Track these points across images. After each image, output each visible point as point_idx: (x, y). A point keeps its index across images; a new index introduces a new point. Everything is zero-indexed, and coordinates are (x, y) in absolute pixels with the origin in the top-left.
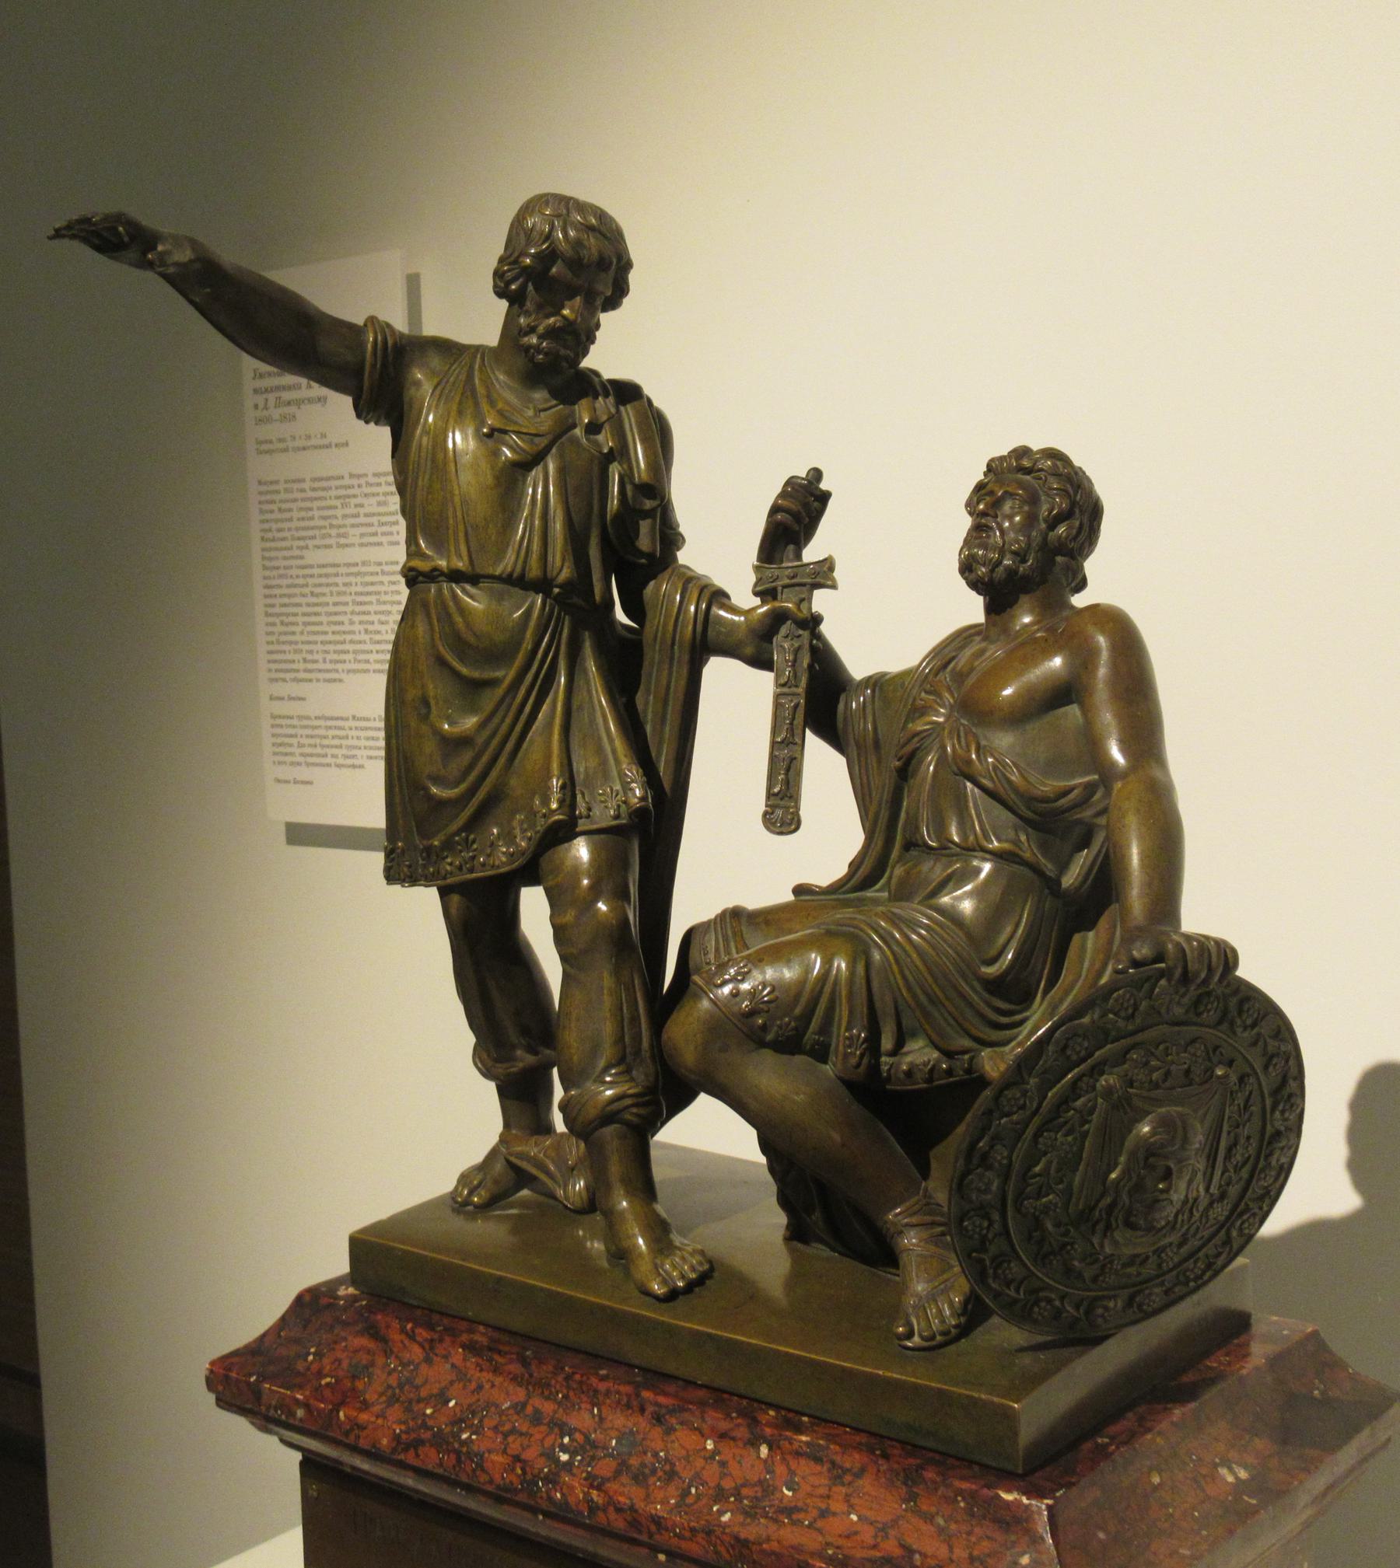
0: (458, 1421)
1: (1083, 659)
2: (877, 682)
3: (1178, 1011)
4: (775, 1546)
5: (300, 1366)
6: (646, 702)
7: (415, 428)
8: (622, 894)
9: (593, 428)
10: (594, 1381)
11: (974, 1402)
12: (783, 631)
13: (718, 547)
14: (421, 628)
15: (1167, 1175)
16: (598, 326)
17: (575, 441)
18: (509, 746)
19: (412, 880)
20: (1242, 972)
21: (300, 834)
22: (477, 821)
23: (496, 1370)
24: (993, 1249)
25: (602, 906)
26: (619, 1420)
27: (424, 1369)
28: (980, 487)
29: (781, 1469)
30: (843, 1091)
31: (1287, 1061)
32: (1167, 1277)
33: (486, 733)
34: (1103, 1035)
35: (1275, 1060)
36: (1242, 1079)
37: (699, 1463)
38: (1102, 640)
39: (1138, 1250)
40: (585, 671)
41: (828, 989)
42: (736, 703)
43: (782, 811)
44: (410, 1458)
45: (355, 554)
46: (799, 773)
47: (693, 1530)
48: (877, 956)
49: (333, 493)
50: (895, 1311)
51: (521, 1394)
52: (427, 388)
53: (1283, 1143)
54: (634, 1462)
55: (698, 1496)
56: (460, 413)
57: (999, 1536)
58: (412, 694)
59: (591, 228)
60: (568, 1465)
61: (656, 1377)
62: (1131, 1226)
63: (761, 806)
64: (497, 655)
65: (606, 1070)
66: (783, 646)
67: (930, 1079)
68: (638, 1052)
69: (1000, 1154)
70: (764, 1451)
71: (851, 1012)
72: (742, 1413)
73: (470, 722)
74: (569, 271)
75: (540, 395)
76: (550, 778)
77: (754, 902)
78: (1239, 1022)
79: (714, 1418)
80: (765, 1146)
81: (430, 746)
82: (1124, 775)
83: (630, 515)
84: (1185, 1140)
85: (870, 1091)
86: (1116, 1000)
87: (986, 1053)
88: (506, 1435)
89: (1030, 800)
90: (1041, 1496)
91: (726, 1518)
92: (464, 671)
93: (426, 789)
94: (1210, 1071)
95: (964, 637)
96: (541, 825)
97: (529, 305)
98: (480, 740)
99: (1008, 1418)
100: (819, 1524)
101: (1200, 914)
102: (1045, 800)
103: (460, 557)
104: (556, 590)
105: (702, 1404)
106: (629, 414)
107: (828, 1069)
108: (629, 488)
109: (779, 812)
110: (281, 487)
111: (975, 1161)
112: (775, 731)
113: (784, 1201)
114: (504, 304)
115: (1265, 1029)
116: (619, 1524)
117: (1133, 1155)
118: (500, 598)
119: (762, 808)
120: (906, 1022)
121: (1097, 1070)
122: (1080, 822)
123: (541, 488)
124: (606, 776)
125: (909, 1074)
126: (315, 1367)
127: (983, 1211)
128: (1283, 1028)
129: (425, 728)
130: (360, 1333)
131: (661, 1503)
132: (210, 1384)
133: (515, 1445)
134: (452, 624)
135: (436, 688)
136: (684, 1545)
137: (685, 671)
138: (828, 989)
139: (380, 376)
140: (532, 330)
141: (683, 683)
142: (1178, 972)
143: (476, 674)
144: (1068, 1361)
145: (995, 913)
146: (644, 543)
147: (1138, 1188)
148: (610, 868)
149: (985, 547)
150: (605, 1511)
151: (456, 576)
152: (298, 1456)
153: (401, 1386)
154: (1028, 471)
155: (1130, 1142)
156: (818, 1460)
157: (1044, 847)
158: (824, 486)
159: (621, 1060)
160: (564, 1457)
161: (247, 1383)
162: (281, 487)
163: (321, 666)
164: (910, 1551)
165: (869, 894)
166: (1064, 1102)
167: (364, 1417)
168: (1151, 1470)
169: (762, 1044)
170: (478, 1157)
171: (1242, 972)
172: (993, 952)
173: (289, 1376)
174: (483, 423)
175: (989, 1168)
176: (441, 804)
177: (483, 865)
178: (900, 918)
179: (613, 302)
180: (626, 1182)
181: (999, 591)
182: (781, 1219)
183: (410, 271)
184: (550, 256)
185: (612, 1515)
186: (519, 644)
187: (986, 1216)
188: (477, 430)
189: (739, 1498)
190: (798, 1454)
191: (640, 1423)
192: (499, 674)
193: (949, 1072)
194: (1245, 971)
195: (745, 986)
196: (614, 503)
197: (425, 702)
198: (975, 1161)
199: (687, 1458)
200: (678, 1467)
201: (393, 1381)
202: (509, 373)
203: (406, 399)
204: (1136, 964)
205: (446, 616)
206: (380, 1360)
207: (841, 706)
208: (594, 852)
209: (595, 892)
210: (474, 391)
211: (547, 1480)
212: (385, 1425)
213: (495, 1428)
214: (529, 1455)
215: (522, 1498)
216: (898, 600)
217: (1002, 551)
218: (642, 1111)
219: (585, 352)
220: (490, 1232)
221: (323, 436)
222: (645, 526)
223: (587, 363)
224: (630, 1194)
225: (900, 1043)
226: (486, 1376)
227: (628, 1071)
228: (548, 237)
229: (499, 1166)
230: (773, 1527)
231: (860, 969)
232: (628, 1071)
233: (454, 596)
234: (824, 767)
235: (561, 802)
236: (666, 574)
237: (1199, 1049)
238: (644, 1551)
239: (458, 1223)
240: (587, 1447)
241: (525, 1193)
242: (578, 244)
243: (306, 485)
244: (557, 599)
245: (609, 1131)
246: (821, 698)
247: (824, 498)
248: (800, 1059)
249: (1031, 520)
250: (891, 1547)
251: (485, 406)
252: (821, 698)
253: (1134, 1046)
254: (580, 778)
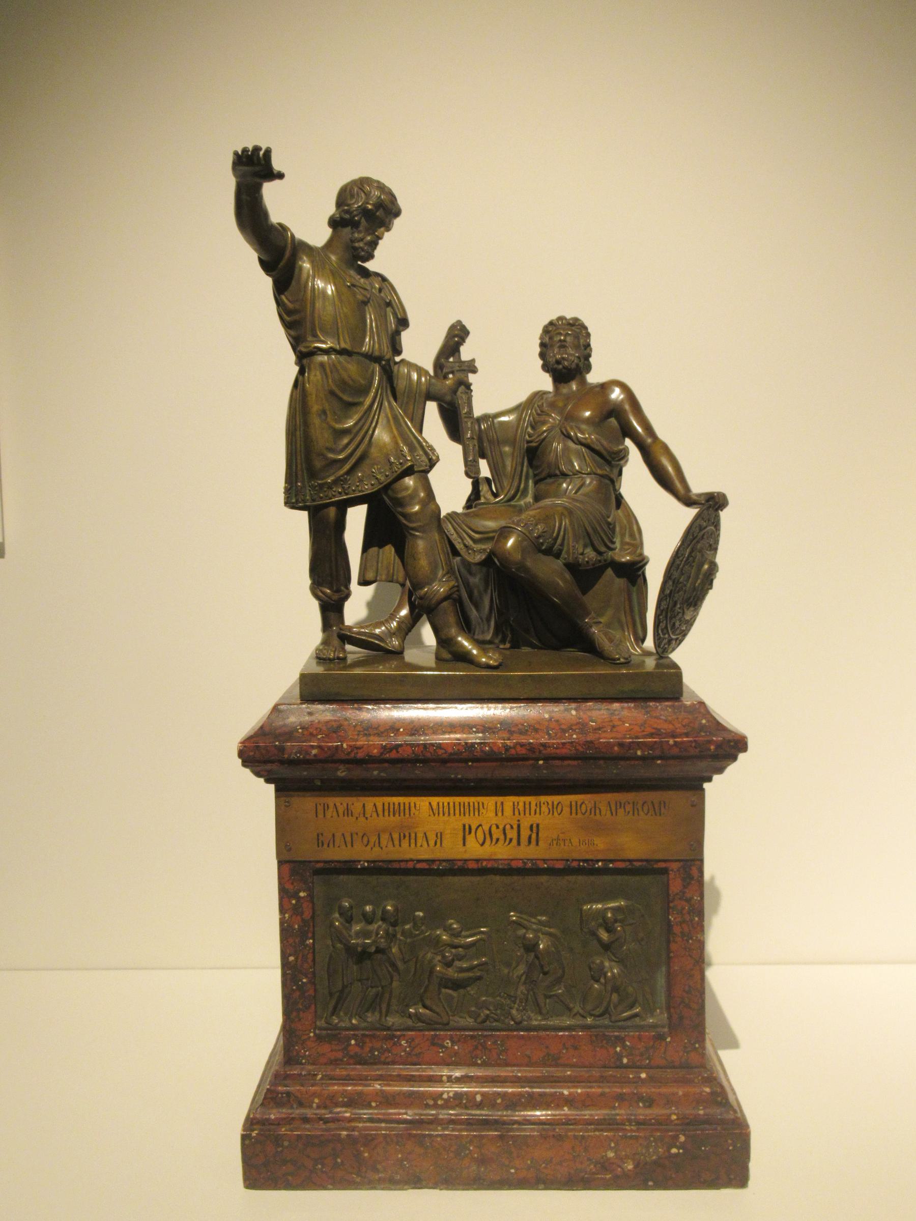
33: (358, 428)
65: (443, 577)
73: (350, 423)
81: (327, 434)
92: (346, 398)
97: (361, 228)
98: (355, 431)
100: (615, 730)
104: (384, 363)
107: (560, 562)
140: (362, 240)
143: (350, 400)
151: (342, 352)
159: (448, 573)
165: (512, 503)
169: (540, 551)
174: (344, 281)
177: (354, 491)
192: (361, 400)
203: (297, 266)
216: (507, 381)
245: (445, 604)
247: (467, 333)
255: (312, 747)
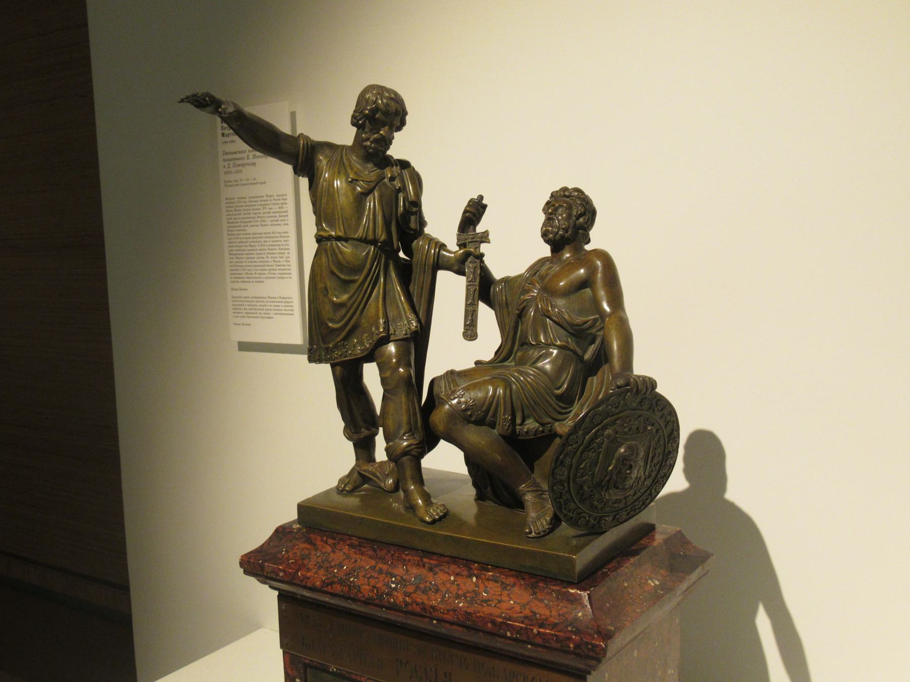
0: (348, 574)
1: (592, 270)
2: (506, 280)
3: (634, 405)
4: (481, 614)
5: (280, 556)
6: (414, 288)
7: (320, 178)
8: (408, 365)
9: (392, 179)
10: (404, 556)
11: (558, 556)
12: (469, 260)
13: (441, 224)
14: (324, 260)
15: (631, 467)
16: (393, 138)
17: (385, 184)
18: (361, 306)
19: (320, 361)
20: (657, 390)
21: (244, 347)
22: (347, 337)
23: (362, 554)
24: (564, 498)
25: (401, 370)
26: (414, 571)
27: (332, 555)
28: (548, 203)
29: (481, 585)
30: (502, 440)
33: (351, 302)
34: (608, 415)
36: (657, 431)
37: (448, 585)
38: (599, 263)
40: (390, 276)
41: (495, 400)
42: (451, 289)
43: (470, 332)
44: (329, 589)
45: (270, 229)
46: (477, 317)
47: (448, 611)
48: (514, 387)
49: (259, 203)
50: (524, 524)
51: (373, 563)
52: (324, 162)
54: (422, 586)
55: (449, 597)
56: (339, 172)
57: (570, 606)
58: (320, 286)
59: (392, 99)
60: (395, 589)
61: (429, 554)
62: (616, 487)
63: (461, 329)
64: (356, 270)
65: (404, 435)
66: (469, 266)
67: (535, 435)
68: (416, 428)
69: (568, 461)
70: (474, 579)
71: (505, 410)
72: (465, 566)
73: (345, 297)
74: (381, 115)
75: (370, 165)
76: (379, 319)
77: (458, 368)
79: (453, 568)
80: (468, 461)
81: (328, 307)
82: (610, 315)
83: (407, 214)
84: (638, 454)
85: (512, 439)
87: (556, 424)
88: (368, 579)
89: (572, 325)
90: (584, 590)
91: (461, 605)
92: (342, 277)
93: (327, 324)
94: (645, 428)
95: (542, 262)
96: (376, 338)
97: (366, 130)
98: (349, 304)
99: (572, 562)
101: (640, 368)
102: (577, 325)
103: (340, 231)
105: (448, 563)
106: (406, 173)
107: (496, 431)
108: (407, 203)
109: (469, 332)
110: (236, 200)
112: (467, 299)
113: (475, 484)
114: (355, 129)
115: (666, 412)
116: (418, 609)
117: (618, 460)
118: (356, 247)
119: (462, 330)
120: (526, 413)
121: (605, 428)
122: (591, 334)
123: (371, 203)
124: (401, 317)
125: (527, 432)
126: (286, 556)
127: (561, 482)
129: (326, 300)
130: (304, 542)
131: (435, 600)
132: (242, 564)
133: (373, 582)
134: (337, 257)
135: (330, 283)
136: (445, 616)
137: (430, 277)
138: (495, 400)
139: (304, 157)
140: (368, 139)
141: (429, 281)
142: (635, 390)
143: (347, 278)
144: (592, 541)
145: (559, 370)
146: (413, 225)
147: (619, 472)
148: (403, 356)
149: (552, 227)
150: (411, 605)
151: (338, 239)
152: (277, 593)
153: (323, 562)
154: (568, 197)
155: (617, 455)
156: (496, 582)
157: (578, 344)
158: (484, 202)
159: (410, 430)
160: (393, 586)
161: (256, 565)
162: (236, 200)
163: (254, 276)
164: (535, 613)
165: (506, 364)
166: (592, 440)
167: (309, 574)
169: (470, 422)
170: (346, 472)
171: (657, 390)
172: (559, 385)
173: (275, 559)
174: (348, 177)
175: (563, 466)
176: (333, 330)
178: (523, 372)
179: (399, 129)
180: (413, 478)
181: (557, 245)
182: (472, 492)
183: (292, 110)
184: (376, 110)
185: (414, 606)
186: (365, 266)
187: (562, 485)
188: (346, 180)
189: (465, 597)
190: (488, 580)
191: (424, 571)
192: (356, 278)
193: (543, 432)
194: (658, 390)
195: (463, 400)
196: (401, 209)
197: (326, 289)
199: (443, 584)
200: (440, 587)
201: (319, 560)
202: (357, 156)
204: (619, 387)
205: (334, 254)
206: (313, 552)
207: (492, 290)
208: (397, 347)
209: (398, 364)
210: (343, 164)
211: (387, 594)
212: (318, 577)
213: (364, 576)
214: (379, 585)
215: (377, 602)
216: (515, 248)
217: (559, 228)
219: (388, 148)
220: (353, 501)
221: (255, 179)
222: (413, 218)
223: (389, 153)
224: (415, 483)
225: (523, 421)
226: (358, 556)
227: (413, 435)
228: (375, 102)
229: (356, 475)
230: (480, 607)
231: (508, 392)
232: (413, 435)
233: (338, 246)
234: (486, 315)
235: (384, 328)
236: (421, 238)
237: (642, 419)
238: (427, 620)
239: (339, 499)
240: (403, 581)
241: (366, 486)
242: (387, 105)
243: (247, 200)
244: (380, 248)
245: (405, 459)
246: (484, 288)
247: (485, 207)
248: (484, 428)
249: (569, 216)
250: (527, 612)
251: (349, 170)
252: (484, 288)
253: (617, 419)
254: (390, 319)
255: (280, 570)
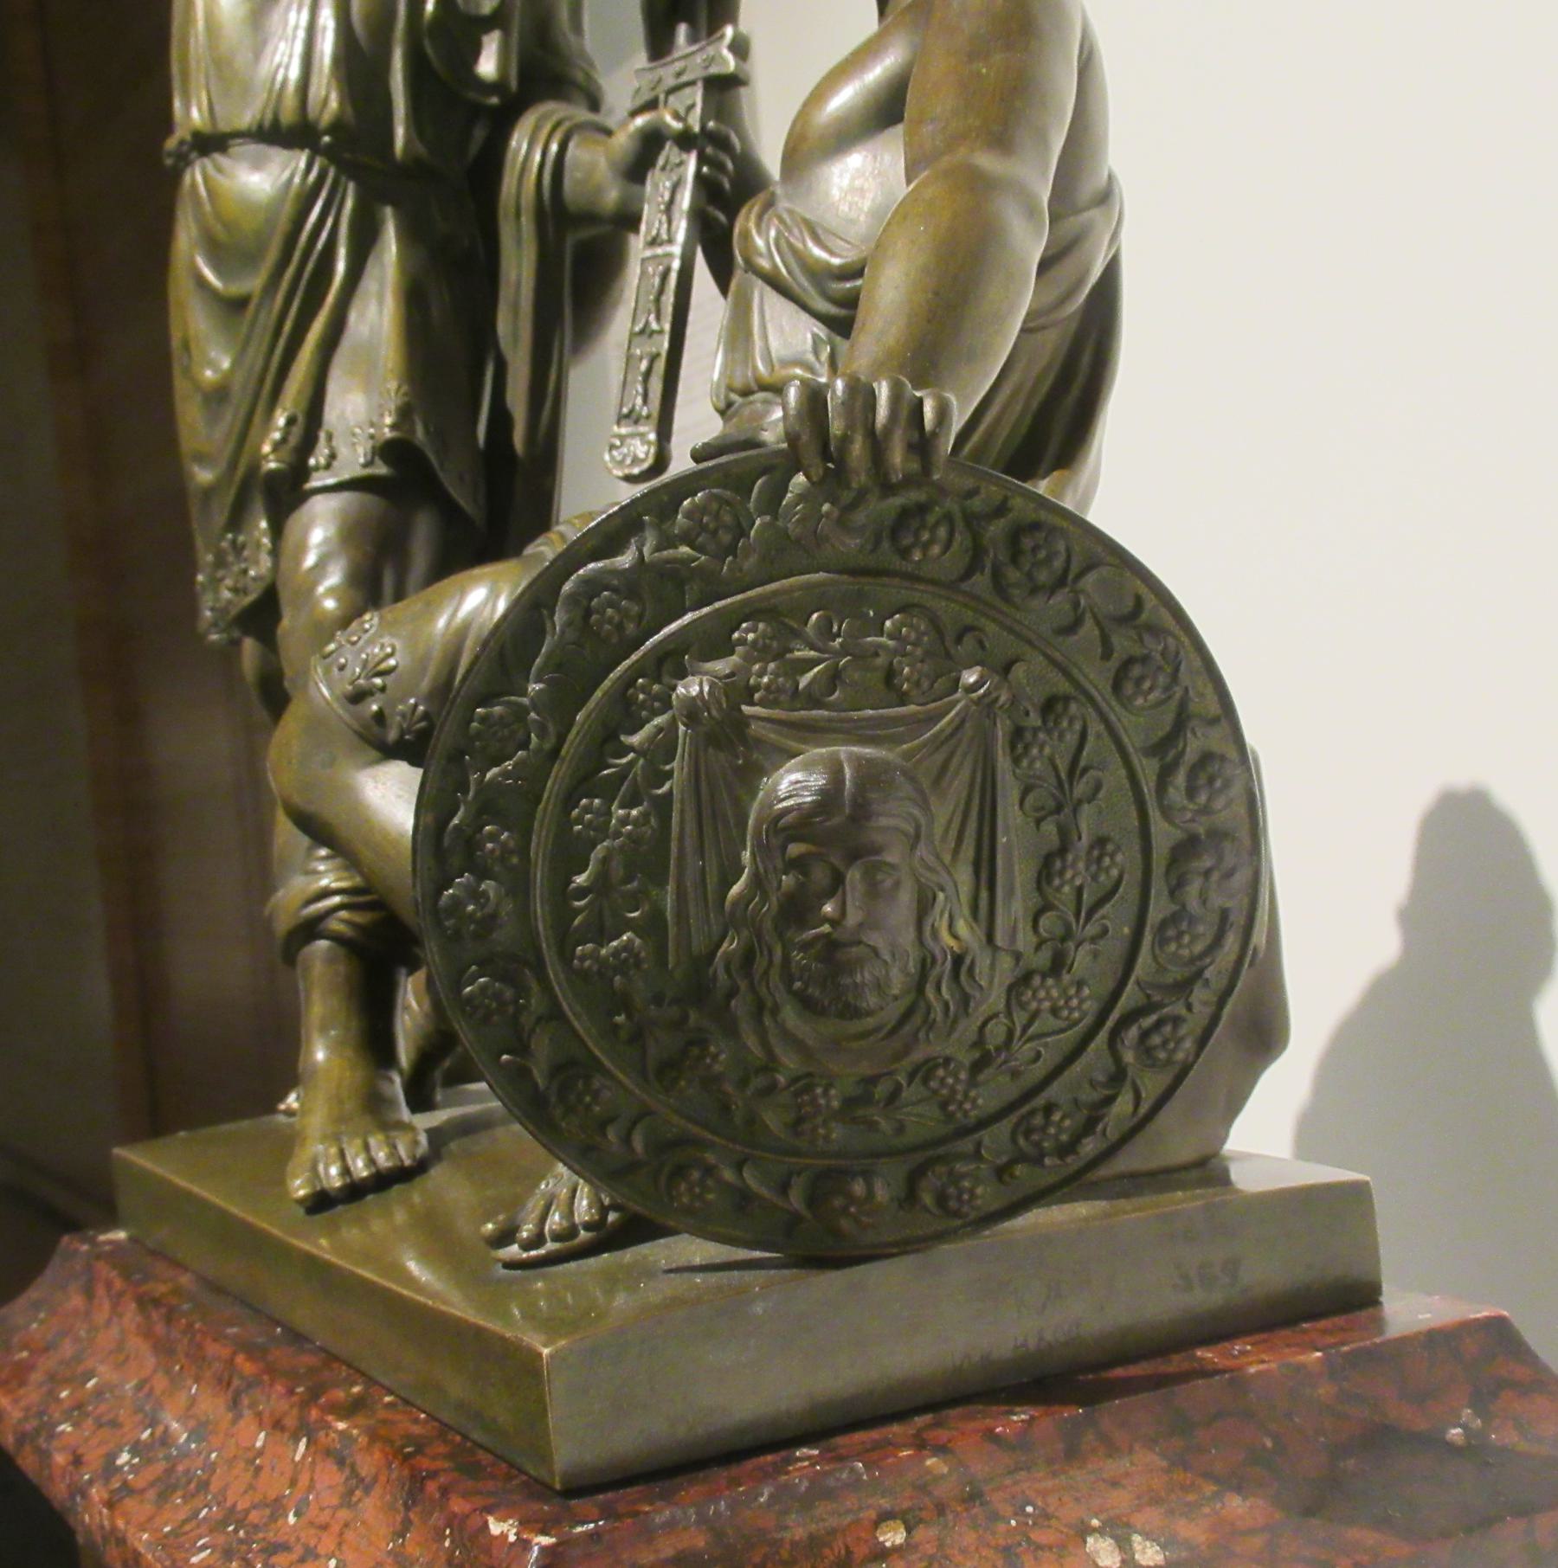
31: (1175, 676)
32: (986, 1136)
35: (1136, 671)
39: (865, 1069)
53: (1207, 862)
69: (495, 838)
78: (1013, 575)
86: (689, 515)
111: (456, 861)
121: (671, 663)
128: (1150, 601)
168: (885, 1517)
175: (483, 874)
198: (456, 861)
218: (360, 918)
244: (331, 153)
